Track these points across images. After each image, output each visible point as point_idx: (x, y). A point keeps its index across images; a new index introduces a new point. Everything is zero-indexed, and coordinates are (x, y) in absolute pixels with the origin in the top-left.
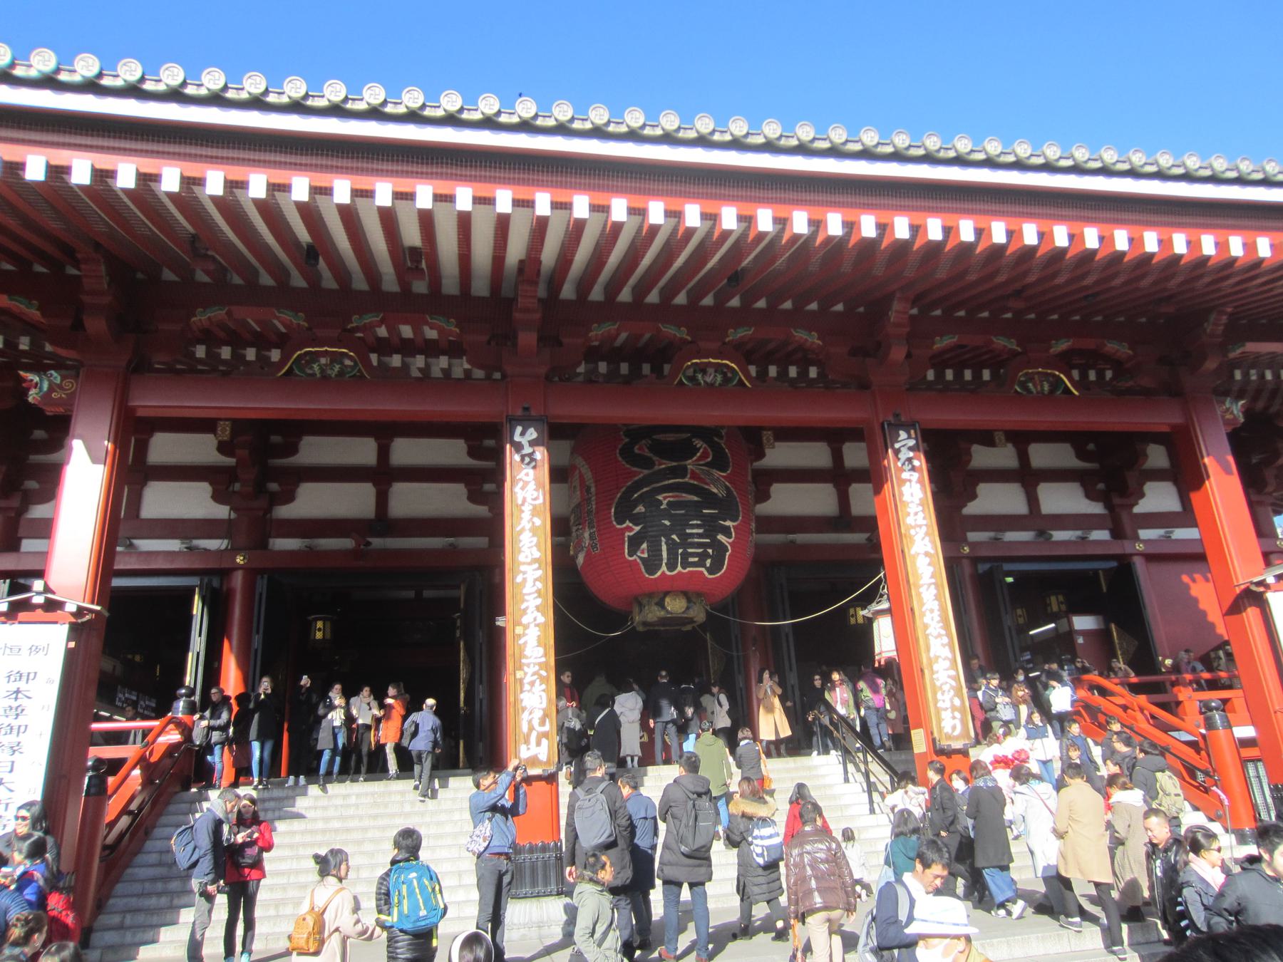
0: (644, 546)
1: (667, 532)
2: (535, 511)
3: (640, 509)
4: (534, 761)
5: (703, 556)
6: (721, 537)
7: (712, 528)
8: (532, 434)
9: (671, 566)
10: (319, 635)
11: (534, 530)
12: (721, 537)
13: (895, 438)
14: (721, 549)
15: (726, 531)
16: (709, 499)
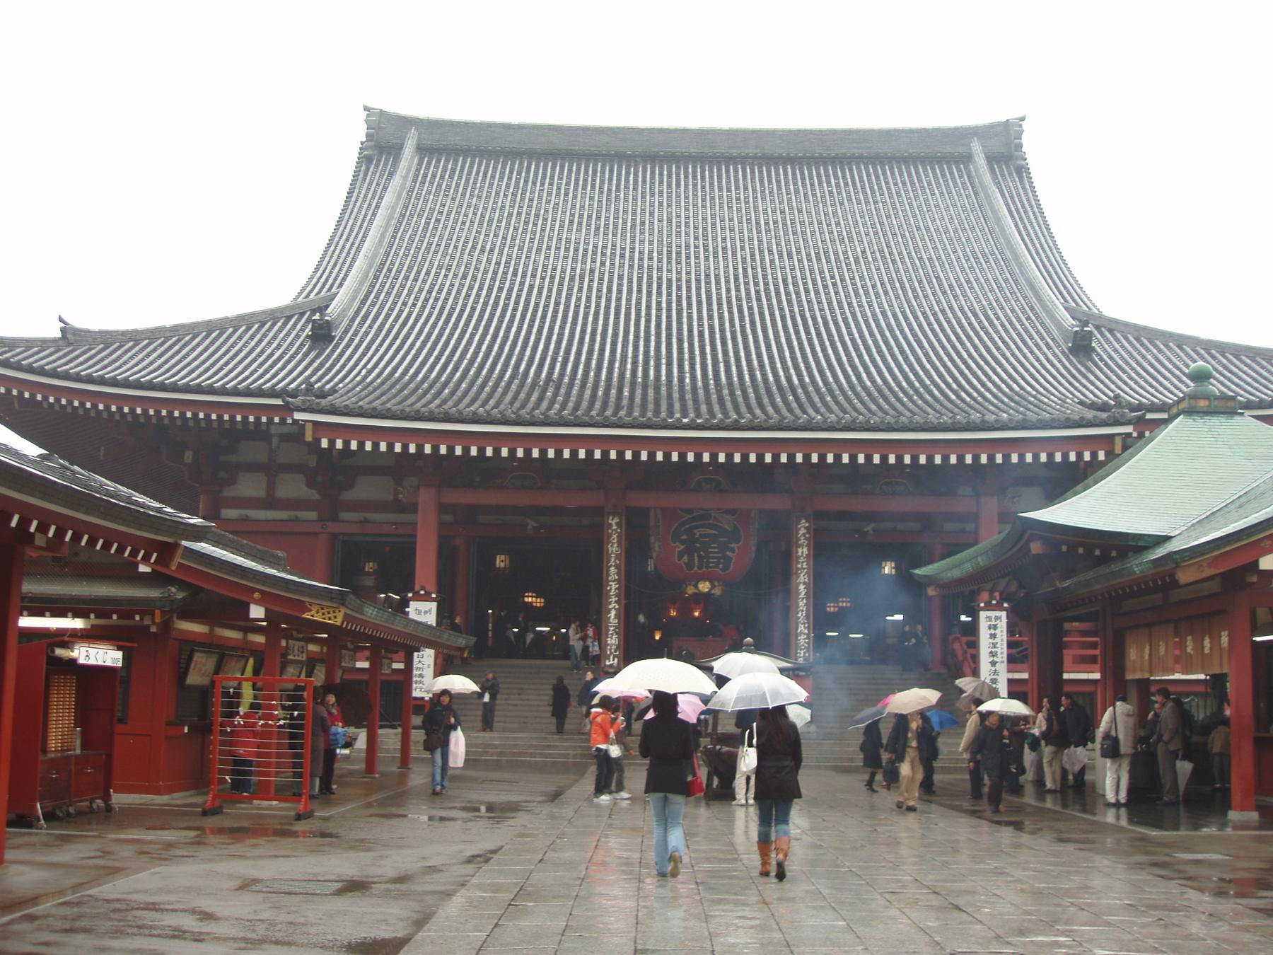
0: (686, 557)
1: (698, 550)
3: (685, 537)
4: (611, 666)
5: (717, 564)
6: (728, 553)
8: (616, 520)
9: (700, 568)
11: (617, 566)
12: (728, 553)
13: (798, 523)
14: (728, 559)
15: (732, 550)
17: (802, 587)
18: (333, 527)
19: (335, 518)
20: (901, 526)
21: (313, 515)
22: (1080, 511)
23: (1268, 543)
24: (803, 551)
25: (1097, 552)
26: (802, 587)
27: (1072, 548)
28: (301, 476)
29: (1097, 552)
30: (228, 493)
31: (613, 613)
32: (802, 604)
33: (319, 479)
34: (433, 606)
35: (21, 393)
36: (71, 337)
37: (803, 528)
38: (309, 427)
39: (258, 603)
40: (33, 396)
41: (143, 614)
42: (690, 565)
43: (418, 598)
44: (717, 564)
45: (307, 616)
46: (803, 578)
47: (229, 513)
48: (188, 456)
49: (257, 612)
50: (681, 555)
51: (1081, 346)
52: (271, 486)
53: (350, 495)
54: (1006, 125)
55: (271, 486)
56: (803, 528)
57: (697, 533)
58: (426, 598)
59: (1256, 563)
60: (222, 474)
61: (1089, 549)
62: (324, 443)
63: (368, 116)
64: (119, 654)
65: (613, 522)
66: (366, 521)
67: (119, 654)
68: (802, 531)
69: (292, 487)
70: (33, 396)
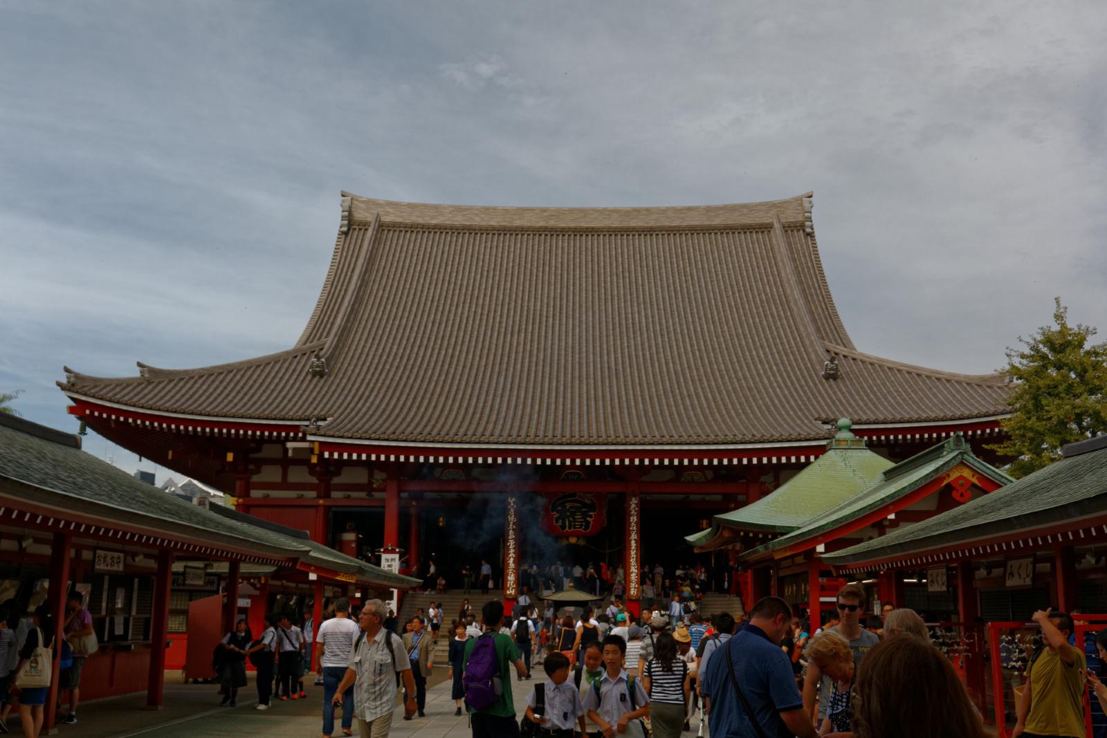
1: (568, 517)
2: (514, 524)
5: (581, 526)
7: (585, 515)
8: (514, 499)
9: (570, 528)
10: (441, 524)
15: (591, 516)
16: (585, 505)
17: (633, 544)
18: (329, 503)
19: (327, 495)
20: (708, 498)
21: (313, 494)
22: (754, 514)
23: (820, 539)
24: (634, 519)
25: (761, 536)
26: (633, 544)
27: (746, 533)
28: (305, 469)
29: (761, 536)
30: (255, 479)
31: (512, 560)
32: (633, 553)
33: (318, 469)
34: (397, 556)
35: (118, 418)
36: (152, 377)
37: (634, 504)
38: (316, 447)
39: (314, 572)
40: (126, 419)
41: (254, 578)
42: (563, 527)
43: (387, 551)
44: (581, 526)
45: (338, 578)
46: (634, 536)
47: (256, 494)
48: (230, 457)
49: (313, 577)
50: (557, 521)
51: (832, 376)
52: (285, 475)
53: (336, 480)
54: (799, 201)
55: (285, 475)
56: (634, 504)
57: (568, 505)
58: (393, 552)
59: (815, 548)
60: (252, 467)
61: (756, 535)
62: (326, 455)
63: (343, 201)
64: (249, 601)
65: (512, 501)
66: (349, 497)
67: (249, 601)
68: (633, 506)
69: (297, 475)
70: (126, 419)
